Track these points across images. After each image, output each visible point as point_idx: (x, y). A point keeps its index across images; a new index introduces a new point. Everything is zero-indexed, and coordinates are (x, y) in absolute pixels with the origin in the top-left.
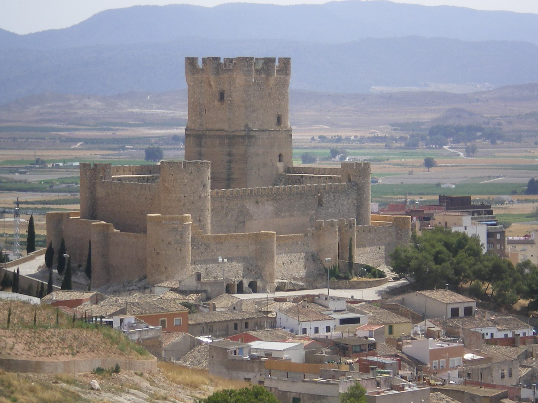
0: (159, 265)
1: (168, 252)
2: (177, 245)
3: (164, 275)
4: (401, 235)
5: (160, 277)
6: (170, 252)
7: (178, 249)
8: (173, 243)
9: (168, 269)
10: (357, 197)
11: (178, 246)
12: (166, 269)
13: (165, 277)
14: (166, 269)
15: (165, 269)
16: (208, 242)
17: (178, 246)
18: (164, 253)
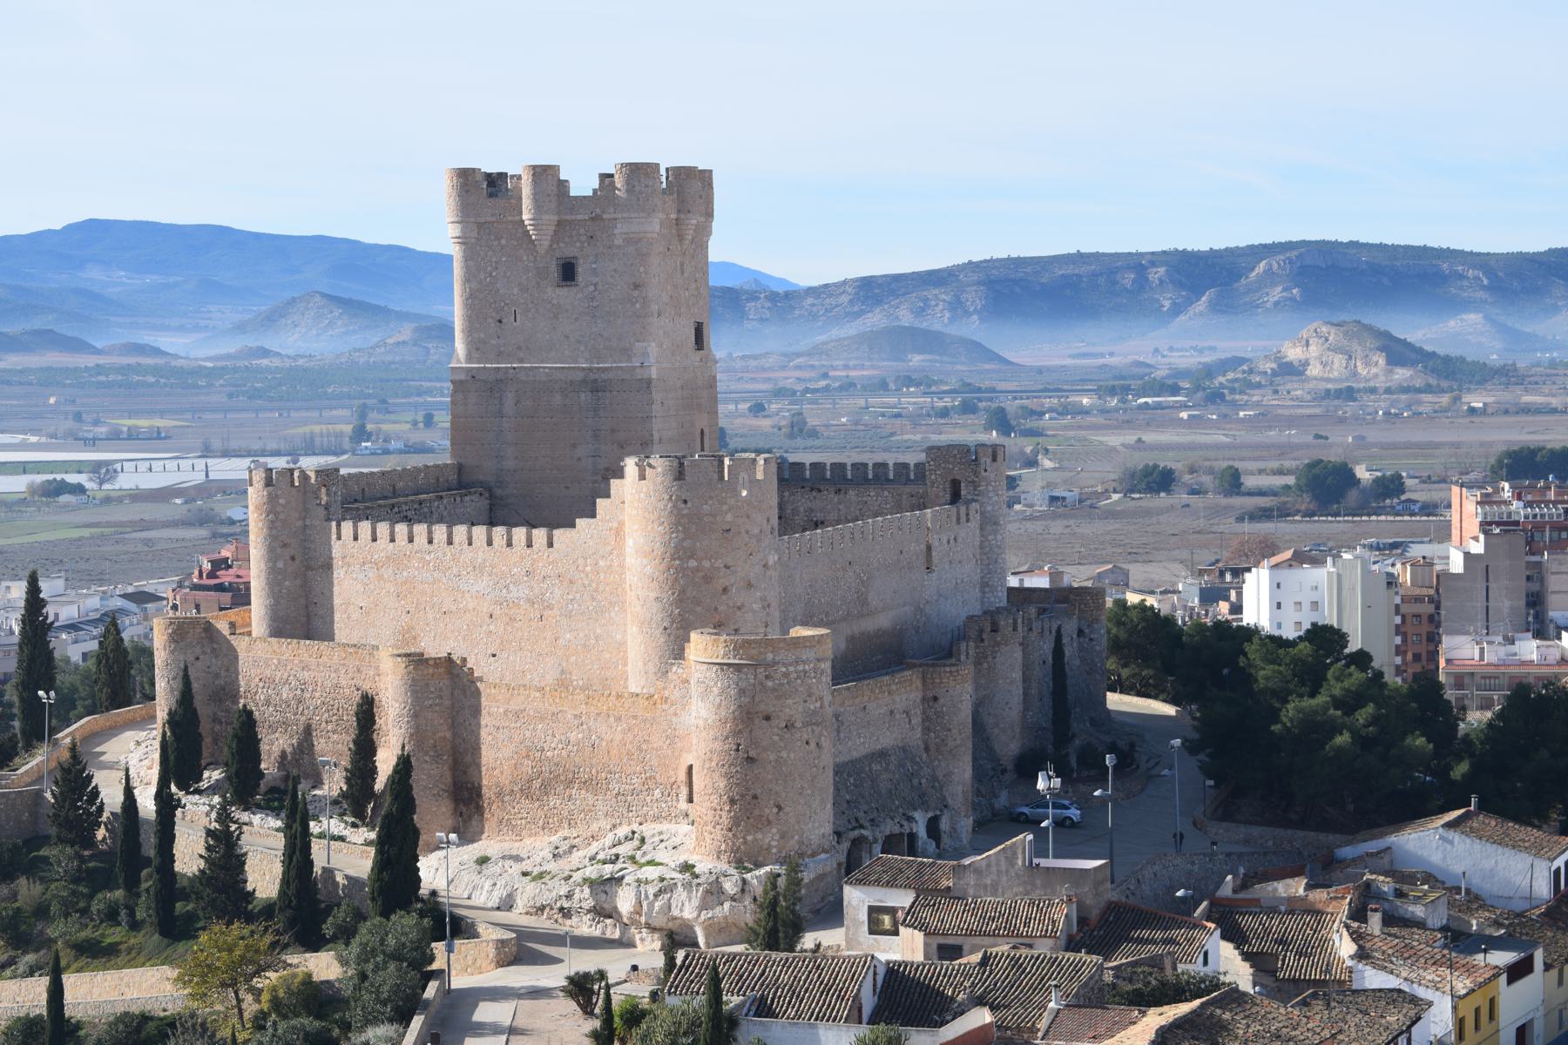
0: (755, 797)
1: (784, 754)
2: (810, 728)
3: (774, 830)
4: (1091, 640)
5: (759, 836)
6: (792, 756)
7: (813, 745)
8: (798, 724)
9: (787, 809)
10: (982, 542)
11: (813, 731)
12: (780, 808)
13: (777, 837)
14: (780, 808)
15: (775, 810)
16: (842, 710)
17: (813, 731)
18: (772, 757)
